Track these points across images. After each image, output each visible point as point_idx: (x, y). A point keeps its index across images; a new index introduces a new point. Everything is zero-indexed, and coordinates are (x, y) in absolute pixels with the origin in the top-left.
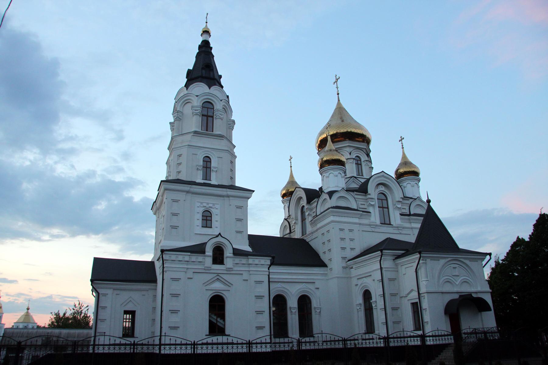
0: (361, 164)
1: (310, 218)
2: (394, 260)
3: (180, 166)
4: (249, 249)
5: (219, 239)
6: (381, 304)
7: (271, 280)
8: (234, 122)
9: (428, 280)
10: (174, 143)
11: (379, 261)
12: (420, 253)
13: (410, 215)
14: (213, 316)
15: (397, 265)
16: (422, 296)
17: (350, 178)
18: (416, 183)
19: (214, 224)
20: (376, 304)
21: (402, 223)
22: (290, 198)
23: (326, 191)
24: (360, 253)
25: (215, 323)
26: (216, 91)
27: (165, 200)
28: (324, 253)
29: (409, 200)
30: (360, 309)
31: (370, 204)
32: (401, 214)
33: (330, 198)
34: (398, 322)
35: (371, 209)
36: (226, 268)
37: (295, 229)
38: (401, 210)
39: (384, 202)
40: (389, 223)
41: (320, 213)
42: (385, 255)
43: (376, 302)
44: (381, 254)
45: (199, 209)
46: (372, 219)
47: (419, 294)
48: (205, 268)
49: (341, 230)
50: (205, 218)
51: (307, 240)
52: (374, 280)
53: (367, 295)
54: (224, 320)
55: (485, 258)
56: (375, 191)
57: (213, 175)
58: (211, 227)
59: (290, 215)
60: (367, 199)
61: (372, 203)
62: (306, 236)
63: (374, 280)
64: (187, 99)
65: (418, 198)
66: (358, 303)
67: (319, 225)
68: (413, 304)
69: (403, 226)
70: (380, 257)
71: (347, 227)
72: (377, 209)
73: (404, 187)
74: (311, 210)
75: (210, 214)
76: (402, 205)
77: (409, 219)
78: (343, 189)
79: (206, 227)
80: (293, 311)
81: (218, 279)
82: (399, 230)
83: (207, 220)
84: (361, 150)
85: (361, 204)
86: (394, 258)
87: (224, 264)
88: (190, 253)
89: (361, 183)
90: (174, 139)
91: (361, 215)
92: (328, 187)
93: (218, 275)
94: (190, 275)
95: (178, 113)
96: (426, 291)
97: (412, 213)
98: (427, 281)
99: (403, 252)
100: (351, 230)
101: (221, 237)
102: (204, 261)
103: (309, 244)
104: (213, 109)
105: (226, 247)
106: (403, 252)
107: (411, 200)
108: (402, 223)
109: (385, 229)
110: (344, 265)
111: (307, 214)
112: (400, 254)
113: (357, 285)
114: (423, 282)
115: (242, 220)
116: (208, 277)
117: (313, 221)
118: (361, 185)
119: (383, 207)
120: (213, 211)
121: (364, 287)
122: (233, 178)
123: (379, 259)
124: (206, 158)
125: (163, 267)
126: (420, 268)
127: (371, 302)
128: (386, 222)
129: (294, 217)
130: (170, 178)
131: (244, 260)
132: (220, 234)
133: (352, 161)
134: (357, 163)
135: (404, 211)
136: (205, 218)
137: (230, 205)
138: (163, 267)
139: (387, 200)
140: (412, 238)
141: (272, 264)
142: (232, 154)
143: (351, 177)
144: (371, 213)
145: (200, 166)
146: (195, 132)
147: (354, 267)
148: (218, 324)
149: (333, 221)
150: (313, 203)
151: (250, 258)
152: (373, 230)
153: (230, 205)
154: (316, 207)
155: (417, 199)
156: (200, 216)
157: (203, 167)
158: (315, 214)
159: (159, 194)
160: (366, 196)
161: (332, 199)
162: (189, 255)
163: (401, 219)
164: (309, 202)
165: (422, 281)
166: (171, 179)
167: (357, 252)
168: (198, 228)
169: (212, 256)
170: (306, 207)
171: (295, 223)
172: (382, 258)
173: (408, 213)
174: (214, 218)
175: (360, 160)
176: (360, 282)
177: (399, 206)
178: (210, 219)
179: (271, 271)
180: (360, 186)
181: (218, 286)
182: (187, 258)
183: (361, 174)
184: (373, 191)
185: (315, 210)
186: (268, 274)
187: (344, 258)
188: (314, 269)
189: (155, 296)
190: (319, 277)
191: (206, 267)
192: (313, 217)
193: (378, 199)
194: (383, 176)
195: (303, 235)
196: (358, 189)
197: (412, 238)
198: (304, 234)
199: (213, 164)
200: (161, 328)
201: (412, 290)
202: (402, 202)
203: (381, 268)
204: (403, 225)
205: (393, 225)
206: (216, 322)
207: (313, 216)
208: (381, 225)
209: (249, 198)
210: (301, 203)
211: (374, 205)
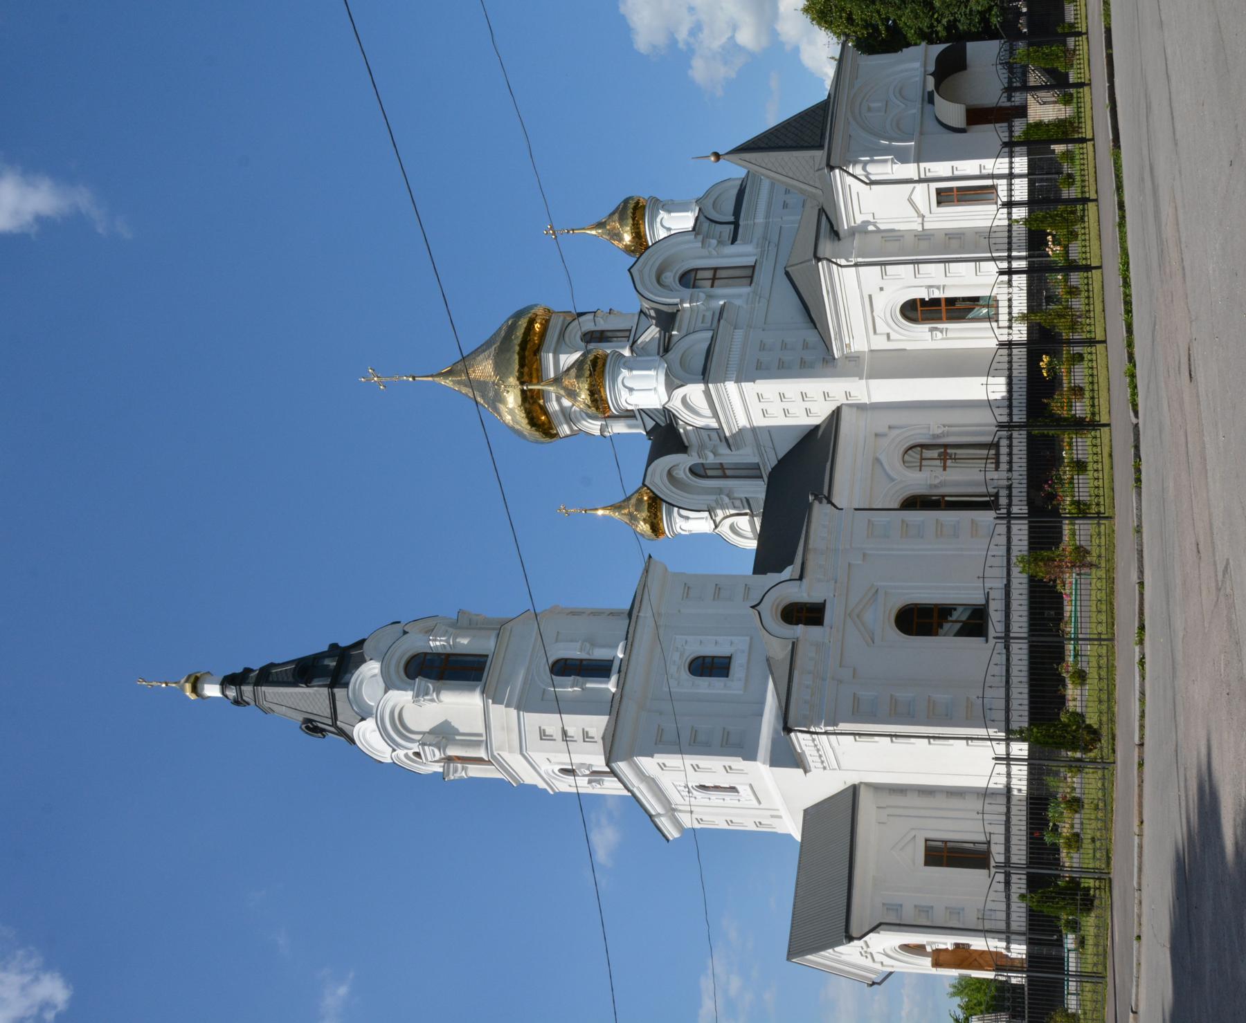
3: (571, 732)
11: (839, 268)
21: (755, 241)
30: (942, 332)
41: (714, 420)
47: (920, 181)
57: (600, 654)
62: (764, 466)
72: (718, 291)
74: (702, 447)
76: (713, 238)
84: (566, 329)
87: (825, 601)
90: (495, 754)
97: (732, 219)
108: (755, 241)
109: (762, 277)
119: (714, 279)
128: (748, 274)
129: (714, 497)
139: (697, 270)
147: (847, 342)
150: (687, 440)
163: (745, 243)
165: (893, 173)
171: (728, 496)
173: (732, 227)
183: (627, 334)
192: (721, 441)
195: (761, 477)
207: (718, 440)
208: (753, 284)
209: (666, 569)
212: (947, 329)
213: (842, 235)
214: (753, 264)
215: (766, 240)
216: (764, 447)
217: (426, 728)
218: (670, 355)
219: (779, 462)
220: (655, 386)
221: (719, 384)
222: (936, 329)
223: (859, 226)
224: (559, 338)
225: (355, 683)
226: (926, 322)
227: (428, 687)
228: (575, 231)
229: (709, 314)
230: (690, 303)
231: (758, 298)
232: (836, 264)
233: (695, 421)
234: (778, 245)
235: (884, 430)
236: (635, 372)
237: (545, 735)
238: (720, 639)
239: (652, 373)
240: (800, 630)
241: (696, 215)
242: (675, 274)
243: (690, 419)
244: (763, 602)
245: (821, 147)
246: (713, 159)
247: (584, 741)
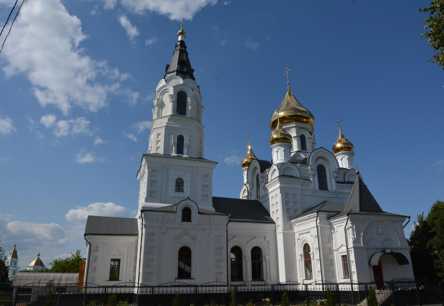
3: (159, 143)
4: (213, 209)
10: (155, 124)
14: (181, 263)
18: (350, 157)
19: (185, 189)
21: (338, 190)
22: (248, 167)
23: (275, 163)
30: (301, 259)
32: (337, 182)
37: (251, 192)
41: (270, 181)
43: (313, 254)
50: (178, 184)
51: (261, 202)
53: (306, 247)
54: (190, 267)
55: (404, 220)
56: (315, 163)
57: (185, 150)
58: (183, 191)
62: (260, 199)
64: (164, 89)
75: (182, 180)
76: (337, 175)
81: (186, 233)
84: (305, 129)
87: (191, 222)
90: (155, 121)
93: (186, 230)
101: (189, 200)
108: (338, 190)
109: (323, 193)
111: (260, 181)
113: (299, 239)
115: (207, 187)
121: (304, 241)
129: (251, 183)
136: (178, 184)
164: (263, 170)
165: (349, 238)
166: (152, 153)
170: (260, 176)
174: (185, 185)
176: (301, 236)
178: (182, 185)
195: (258, 197)
198: (259, 196)
199: (186, 141)
201: (342, 245)
206: (183, 268)
208: (319, 190)
209: (213, 169)
210: (257, 171)
212: (302, 261)
213: (329, 220)
215: (338, 193)
216: (264, 198)
217: (163, 100)
218: (290, 164)
219: (261, 204)
220: (279, 159)
221: (278, 181)
222: (302, 257)
223: (333, 227)
224: (302, 127)
225: (176, 77)
226: (304, 252)
227: (174, 98)
228: (340, 129)
229: (307, 176)
230: (310, 169)
231: (314, 192)
233: (269, 175)
235: (267, 239)
236: (283, 152)
237: (159, 135)
238: (189, 188)
239: (283, 158)
240: (180, 214)
241: (347, 169)
242: (322, 163)
243: (270, 172)
244: (190, 201)
245: (361, 210)
246: (357, 171)
247: (157, 147)
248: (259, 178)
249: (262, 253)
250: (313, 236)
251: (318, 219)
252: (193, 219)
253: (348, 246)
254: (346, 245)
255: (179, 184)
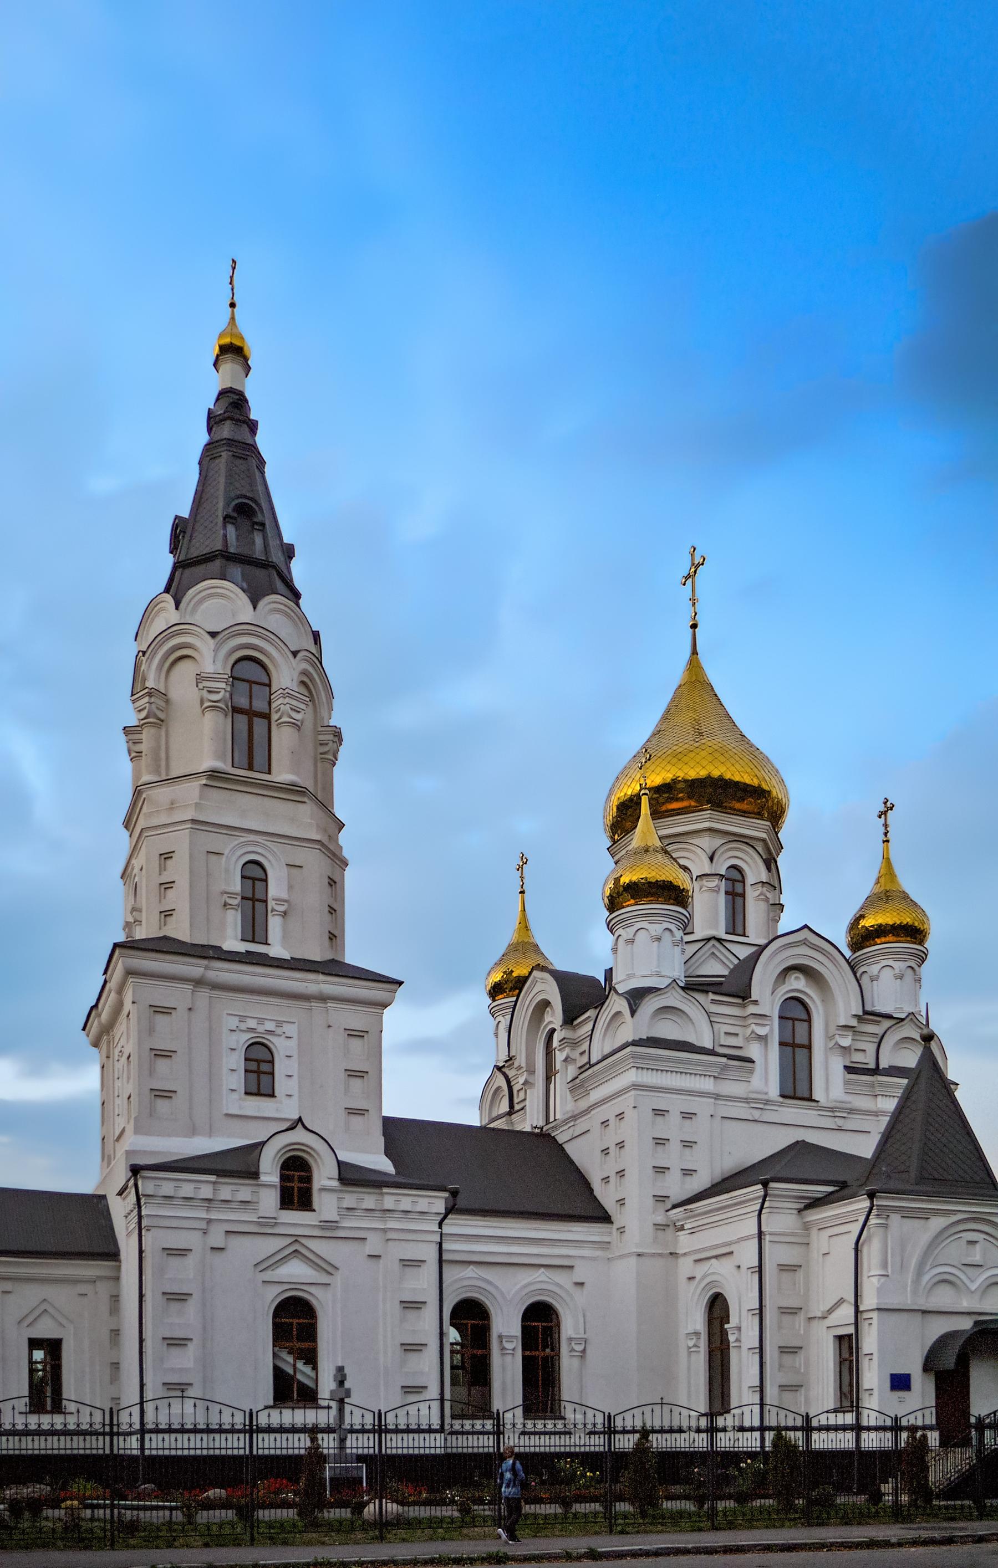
0: (743, 895)
1: (572, 1071)
2: (800, 1211)
4: (386, 1165)
5: (299, 1136)
6: (750, 1337)
7: (445, 1257)
8: (337, 735)
9: (888, 1276)
10: (145, 810)
11: (757, 1212)
12: (871, 1196)
13: (876, 1071)
15: (807, 1227)
16: (865, 1319)
17: (703, 943)
19: (281, 1085)
20: (740, 1334)
21: (849, 1098)
22: (514, 999)
23: (621, 988)
24: (709, 1185)
25: (288, 1374)
26: (278, 616)
27: (128, 1006)
28: (606, 1180)
29: (879, 1022)
31: (753, 1032)
32: (849, 1069)
33: (633, 1013)
34: (793, 1388)
35: (754, 1051)
36: (321, 1222)
38: (850, 1053)
39: (801, 1028)
40: (807, 1095)
42: (771, 1195)
43: (739, 1329)
44: (763, 1193)
45: (234, 1036)
46: (756, 1081)
47: (857, 1311)
48: (260, 1220)
49: (659, 1113)
50: (253, 1066)
51: (561, 1139)
52: (739, 1267)
54: (315, 1368)
58: (272, 1095)
59: (512, 1054)
60: (745, 1017)
61: (762, 1031)
63: (739, 1267)
65: (911, 1017)
66: (690, 1330)
67: (595, 1096)
68: (840, 1338)
69: (848, 1106)
70: (761, 1201)
71: (675, 1104)
73: (873, 979)
74: (574, 1044)
77: (872, 1085)
78: (674, 985)
79: (259, 1094)
80: (509, 1346)
81: (296, 1251)
82: (836, 1119)
83: (258, 1072)
85: (726, 1033)
86: (802, 1206)
87: (314, 1211)
88: (215, 1176)
89: (736, 961)
91: (725, 1068)
92: (630, 977)
93: (296, 1240)
94: (216, 1238)
95: (153, 700)
96: (877, 1303)
97: (884, 1064)
98: (883, 1279)
99: (830, 1189)
100: (688, 1116)
102: (255, 1200)
103: (563, 1149)
104: (269, 685)
105: (315, 1155)
106: (830, 1189)
107: (887, 1023)
109: (793, 1112)
110: (660, 1219)
111: (559, 1057)
112: (820, 1196)
114: (871, 1278)
116: (271, 1245)
117: (578, 1081)
118: (736, 966)
119: (794, 1045)
120: (280, 1046)
122: (334, 937)
123: (758, 1207)
124: (249, 865)
125: (140, 1217)
126: (869, 1238)
127: (726, 1329)
130: (140, 933)
131: (369, 1200)
132: (300, 1119)
133: (714, 883)
134: (731, 890)
135: (858, 1057)
136: (253, 1066)
137: (329, 1026)
138: (140, 1217)
139: (809, 1021)
140: (865, 1147)
141: (451, 1210)
142: (334, 854)
143: (709, 940)
144: (753, 1062)
145: (232, 895)
146: (214, 774)
148: (299, 1377)
149: (636, 1087)
150: (580, 1023)
151: (387, 1193)
152: (756, 1115)
153: (329, 1026)
154: (591, 1035)
155: (908, 1019)
156: (237, 1061)
157: (243, 898)
158: (585, 1059)
159: (108, 986)
160: (744, 1006)
161: (634, 1017)
162: (214, 1183)
163: (847, 1083)
167: (701, 1182)
168: (235, 1096)
169: (278, 1184)
171: (526, 1083)
172: (766, 1205)
174: (280, 1068)
175: (743, 882)
177: (846, 1042)
179: (446, 1229)
180: (732, 971)
181: (296, 1271)
182: (206, 1192)
183: (740, 931)
184: (769, 991)
185: (585, 1046)
186: (439, 1240)
187: (660, 1199)
188: (574, 1229)
189: (115, 1299)
190: (586, 1252)
191: (262, 1217)
192: (580, 1068)
193: (780, 1017)
194: (805, 942)
195: (548, 1122)
196: (723, 979)
197: (865, 1147)
200: (142, 1386)
201: (841, 1301)
202: (855, 1029)
203: (760, 1234)
204: (850, 1103)
205: (818, 1101)
206: (291, 1371)
208: (781, 1099)
209: (385, 1005)
210: (547, 1018)
211: (766, 1035)
214: (813, 1098)
232: (762, 1207)
233: (599, 1031)
234: (840, 1129)
244: (308, 1132)
248: (555, 1043)
249: (558, 1325)
250: (744, 1268)
251: (765, 1206)
252: (317, 1199)
253: (861, 1303)
254: (852, 1300)
255: (259, 1065)
